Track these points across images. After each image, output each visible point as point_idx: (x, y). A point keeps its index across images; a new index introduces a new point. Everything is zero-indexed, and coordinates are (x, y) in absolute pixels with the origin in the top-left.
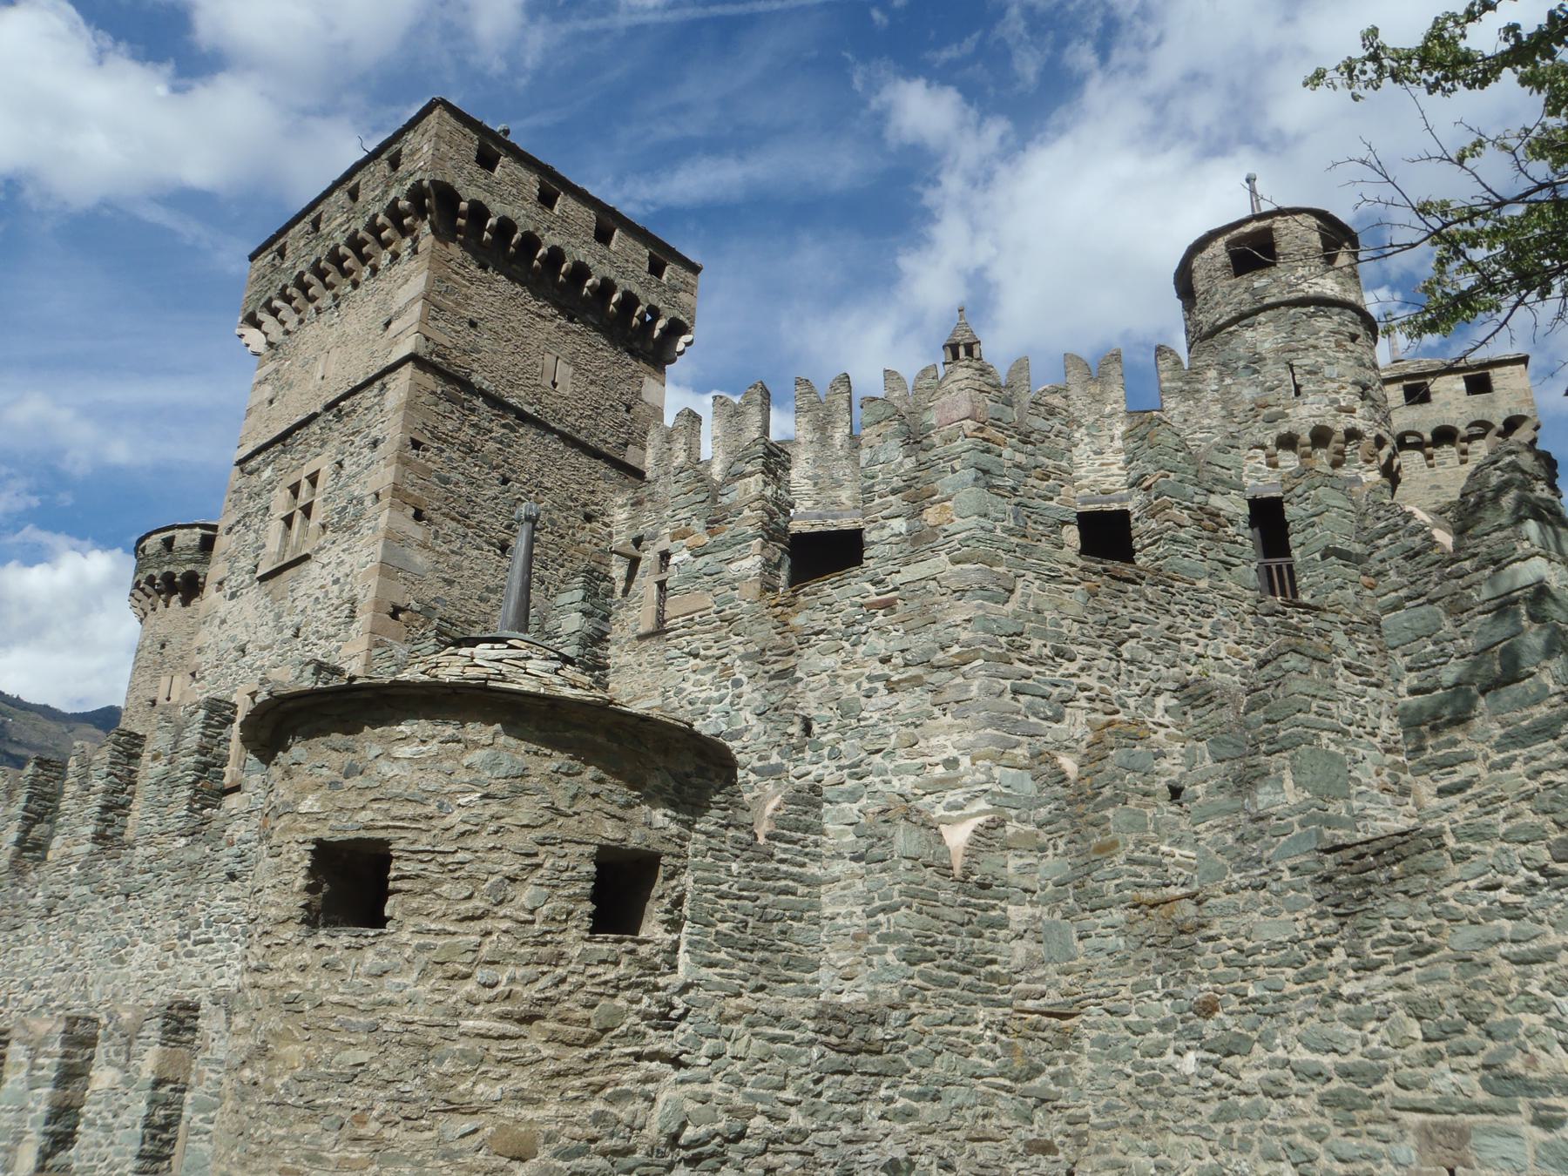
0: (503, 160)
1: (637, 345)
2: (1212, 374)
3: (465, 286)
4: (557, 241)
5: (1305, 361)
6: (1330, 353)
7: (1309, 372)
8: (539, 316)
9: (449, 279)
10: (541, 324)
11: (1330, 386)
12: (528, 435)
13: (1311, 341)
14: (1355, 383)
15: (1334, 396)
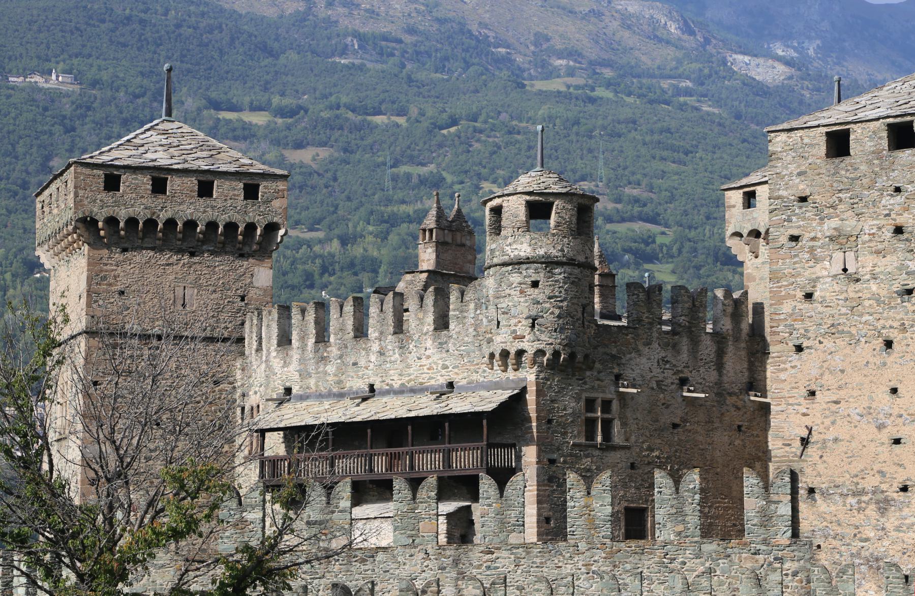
0: (123, 178)
1: (246, 249)
2: (472, 306)
3: (113, 270)
4: (169, 215)
5: (504, 305)
6: (516, 299)
7: (504, 313)
8: (168, 265)
9: (102, 271)
10: (169, 270)
11: (513, 321)
12: (167, 348)
13: (508, 291)
14: (527, 318)
15: (514, 328)
